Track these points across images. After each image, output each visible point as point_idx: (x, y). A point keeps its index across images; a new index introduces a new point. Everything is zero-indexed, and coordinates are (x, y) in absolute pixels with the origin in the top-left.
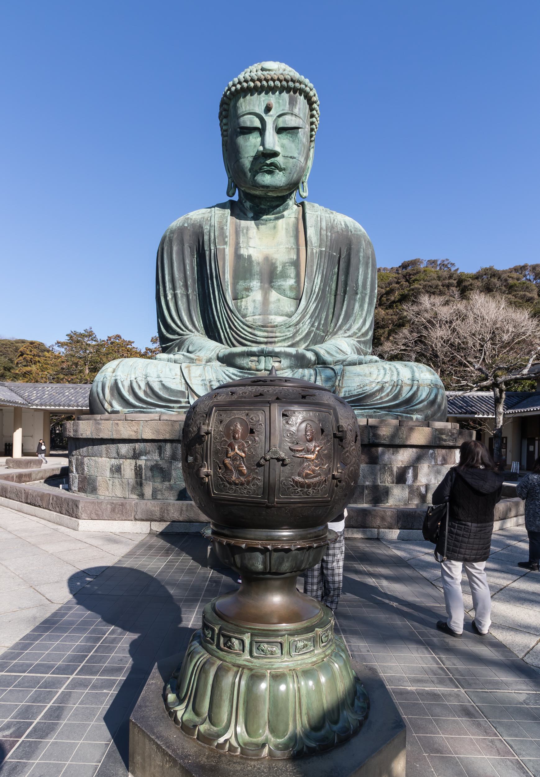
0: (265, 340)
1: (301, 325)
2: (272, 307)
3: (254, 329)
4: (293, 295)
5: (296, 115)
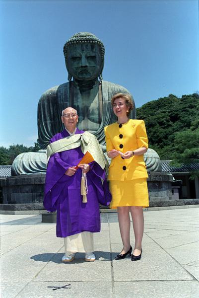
1: (101, 134)
5: (94, 52)
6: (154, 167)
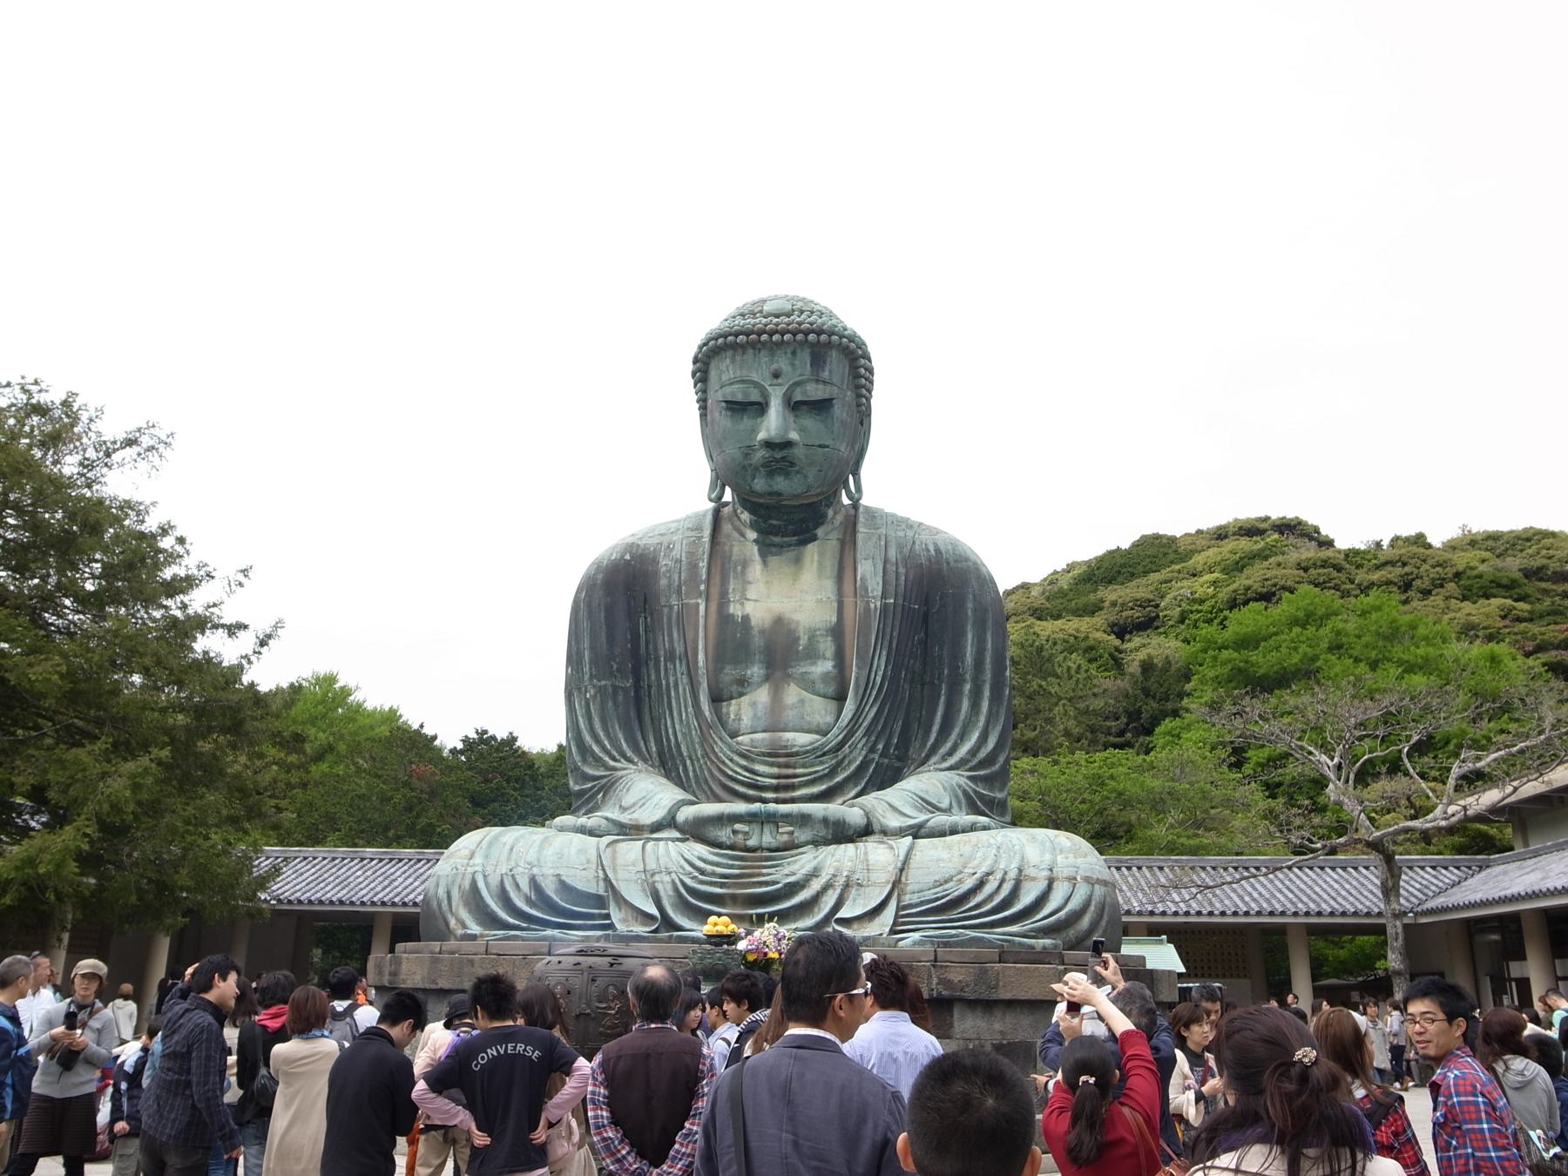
2: (790, 715)
3: (753, 761)
4: (831, 690)
5: (825, 382)
6: (1086, 922)
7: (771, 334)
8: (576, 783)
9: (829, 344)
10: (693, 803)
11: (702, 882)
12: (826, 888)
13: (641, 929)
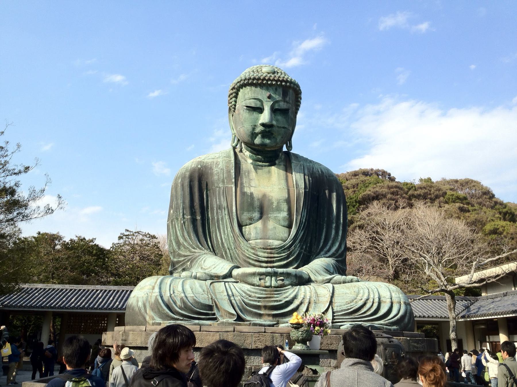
0: (266, 259)
2: (270, 233)
4: (286, 224)
5: (287, 102)
7: (267, 80)
8: (174, 257)
9: (290, 87)
10: (238, 267)
11: (250, 300)
12: (301, 303)
13: (231, 320)
